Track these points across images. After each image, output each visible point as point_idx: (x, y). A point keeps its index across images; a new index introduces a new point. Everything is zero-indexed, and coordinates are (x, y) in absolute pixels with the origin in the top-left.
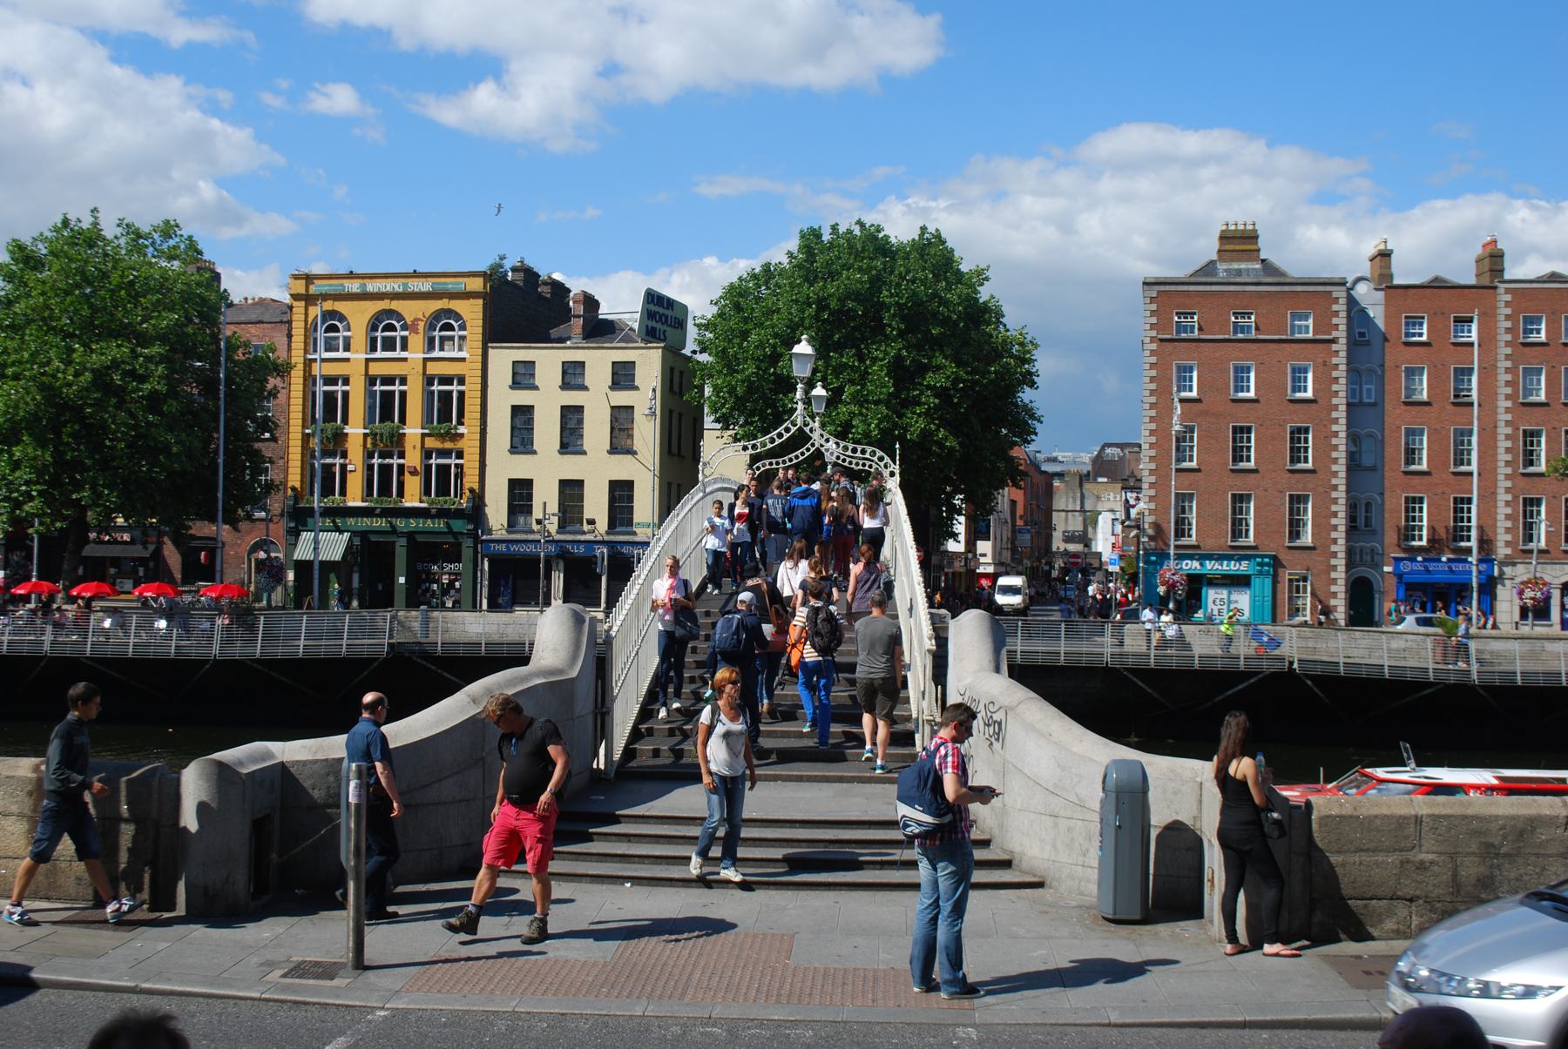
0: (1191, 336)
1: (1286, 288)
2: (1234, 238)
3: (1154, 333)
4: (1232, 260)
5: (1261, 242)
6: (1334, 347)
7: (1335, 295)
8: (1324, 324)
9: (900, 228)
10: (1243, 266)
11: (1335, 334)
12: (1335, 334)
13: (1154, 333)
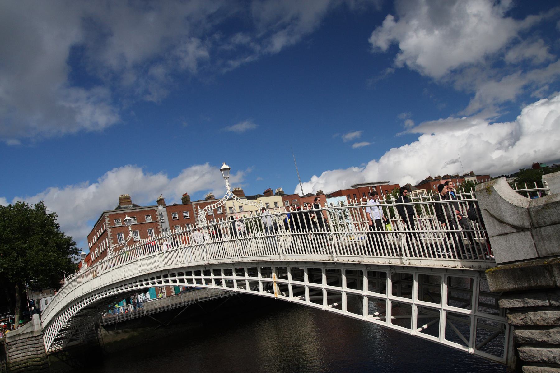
0: (120, 225)
1: (143, 209)
2: (124, 199)
3: (110, 226)
4: (126, 205)
5: (131, 199)
6: (158, 223)
7: (156, 210)
8: (154, 218)
9: (31, 202)
10: (128, 206)
11: (158, 220)
12: (158, 220)
13: (110, 226)
